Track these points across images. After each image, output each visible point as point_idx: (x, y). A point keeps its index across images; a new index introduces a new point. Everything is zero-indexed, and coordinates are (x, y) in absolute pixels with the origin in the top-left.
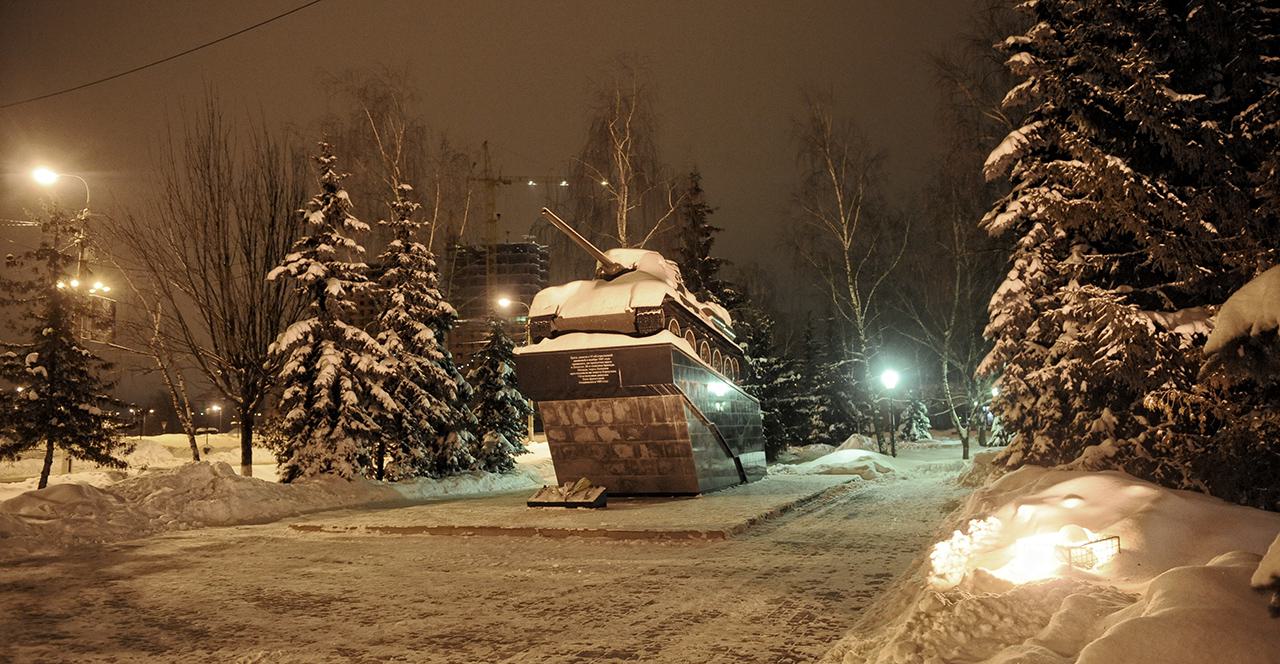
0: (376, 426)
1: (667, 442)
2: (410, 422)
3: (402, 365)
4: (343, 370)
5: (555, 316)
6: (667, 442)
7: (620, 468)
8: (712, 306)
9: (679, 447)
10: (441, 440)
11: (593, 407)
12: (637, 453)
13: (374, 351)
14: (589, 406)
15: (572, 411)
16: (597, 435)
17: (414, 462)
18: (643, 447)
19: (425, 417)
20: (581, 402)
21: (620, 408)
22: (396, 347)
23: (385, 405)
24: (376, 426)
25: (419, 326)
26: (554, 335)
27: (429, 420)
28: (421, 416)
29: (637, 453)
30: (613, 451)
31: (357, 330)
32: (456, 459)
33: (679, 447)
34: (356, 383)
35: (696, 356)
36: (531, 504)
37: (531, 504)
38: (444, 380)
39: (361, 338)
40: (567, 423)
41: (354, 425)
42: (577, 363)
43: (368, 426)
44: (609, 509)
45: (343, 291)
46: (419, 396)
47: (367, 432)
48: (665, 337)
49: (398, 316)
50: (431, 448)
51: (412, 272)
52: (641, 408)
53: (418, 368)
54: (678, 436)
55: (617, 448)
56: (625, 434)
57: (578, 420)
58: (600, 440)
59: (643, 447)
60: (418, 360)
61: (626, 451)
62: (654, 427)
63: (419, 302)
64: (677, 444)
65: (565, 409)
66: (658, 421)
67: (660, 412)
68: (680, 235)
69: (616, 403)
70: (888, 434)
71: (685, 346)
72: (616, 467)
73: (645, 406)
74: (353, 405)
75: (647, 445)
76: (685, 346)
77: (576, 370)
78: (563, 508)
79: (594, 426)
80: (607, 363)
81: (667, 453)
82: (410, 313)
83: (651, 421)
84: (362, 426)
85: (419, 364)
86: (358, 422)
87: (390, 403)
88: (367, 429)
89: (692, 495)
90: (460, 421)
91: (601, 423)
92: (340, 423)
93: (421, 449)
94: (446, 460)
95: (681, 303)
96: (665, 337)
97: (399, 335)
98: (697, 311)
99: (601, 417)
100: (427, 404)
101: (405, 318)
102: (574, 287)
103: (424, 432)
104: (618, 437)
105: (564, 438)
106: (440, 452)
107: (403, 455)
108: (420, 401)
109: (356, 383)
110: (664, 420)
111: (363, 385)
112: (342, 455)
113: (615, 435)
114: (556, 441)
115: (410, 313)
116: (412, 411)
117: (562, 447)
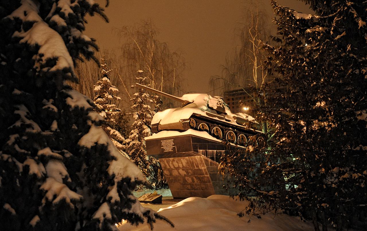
1: (202, 176)
6: (202, 176)
7: (189, 187)
11: (175, 161)
15: (169, 163)
19: (149, 164)
20: (171, 159)
21: (184, 161)
28: (148, 164)
30: (185, 180)
31: (114, 130)
33: (206, 178)
39: (115, 134)
40: (169, 168)
42: (163, 143)
44: (162, 204)
52: (190, 162)
54: (205, 174)
55: (186, 178)
56: (188, 173)
58: (181, 175)
59: (194, 178)
61: (189, 180)
62: (196, 169)
64: (205, 177)
65: (167, 162)
66: (197, 167)
67: (196, 163)
69: (182, 159)
72: (188, 186)
73: (191, 161)
75: (195, 177)
78: (144, 203)
79: (178, 169)
80: (171, 142)
83: (194, 167)
95: (207, 116)
96: (190, 132)
99: (179, 165)
102: (168, 111)
104: (185, 173)
105: (169, 174)
110: (198, 167)
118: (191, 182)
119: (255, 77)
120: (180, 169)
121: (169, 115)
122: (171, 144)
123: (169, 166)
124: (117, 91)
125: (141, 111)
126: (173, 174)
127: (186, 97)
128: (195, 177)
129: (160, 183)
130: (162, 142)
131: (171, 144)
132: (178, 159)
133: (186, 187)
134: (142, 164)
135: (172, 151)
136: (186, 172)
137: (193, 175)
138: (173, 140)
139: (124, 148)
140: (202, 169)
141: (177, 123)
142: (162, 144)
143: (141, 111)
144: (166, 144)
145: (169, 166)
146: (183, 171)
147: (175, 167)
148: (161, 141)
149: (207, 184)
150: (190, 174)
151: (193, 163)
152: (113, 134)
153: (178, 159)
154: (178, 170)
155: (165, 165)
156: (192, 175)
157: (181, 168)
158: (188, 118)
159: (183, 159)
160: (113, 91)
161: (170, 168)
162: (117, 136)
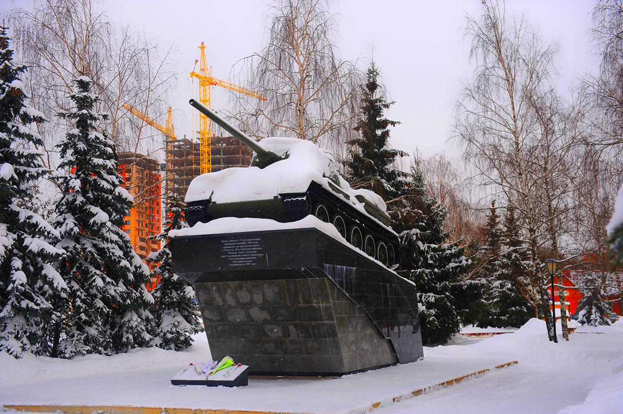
0: (47, 305)
1: (314, 323)
2: (83, 301)
3: (78, 246)
4: (15, 251)
5: (209, 201)
7: (271, 347)
8: (362, 192)
9: (325, 328)
10: (118, 320)
12: (286, 333)
13: (46, 233)
14: (241, 288)
16: (248, 315)
17: (87, 341)
18: (292, 328)
19: (100, 296)
20: (232, 284)
22: (72, 229)
23: (55, 285)
24: (47, 305)
25: (94, 209)
26: (206, 220)
27: (104, 299)
28: (95, 296)
29: (286, 333)
30: (264, 331)
32: (131, 337)
34: (28, 264)
35: (344, 241)
36: (175, 383)
37: (175, 383)
38: (120, 262)
39: (33, 221)
40: (221, 303)
41: (24, 304)
43: (37, 305)
45: (16, 177)
46: (93, 276)
47: (37, 310)
48: (310, 221)
49: (75, 200)
50: (108, 327)
51: (90, 159)
53: (93, 250)
55: (267, 328)
57: (231, 302)
59: (292, 328)
60: (95, 242)
63: (96, 187)
68: (95, 100)
70: (397, 327)
71: (330, 229)
72: (267, 346)
74: (22, 285)
75: (296, 326)
76: (330, 229)
77: (226, 253)
81: (314, 334)
82: (88, 198)
83: (298, 302)
84: (32, 305)
85: (95, 246)
86: (27, 301)
87: (60, 282)
88: (35, 307)
89: (339, 375)
90: (136, 300)
91: (252, 304)
92: (10, 302)
93: (95, 326)
94: (122, 337)
95: (330, 189)
96: (310, 221)
97: (76, 219)
98: (347, 197)
99: (252, 298)
100: (99, 282)
101: (82, 202)
103: (98, 311)
105: (218, 318)
106: (117, 329)
107: (76, 333)
108: (94, 281)
109: (28, 264)
110: (310, 302)
111: (35, 265)
112: (11, 333)
113: (265, 315)
114: (211, 320)
115: (88, 198)
116: (87, 291)
117: (216, 328)
118: (279, 337)
122: (254, 249)
123: (224, 300)
125: (82, 173)
131: (254, 249)
132: (253, 283)
134: (85, 296)
136: (270, 313)
140: (319, 308)
142: (225, 247)
143: (82, 173)
145: (224, 300)
146: (263, 310)
150: (280, 318)
152: (25, 221)
154: (248, 308)
161: (224, 305)
162: (39, 227)
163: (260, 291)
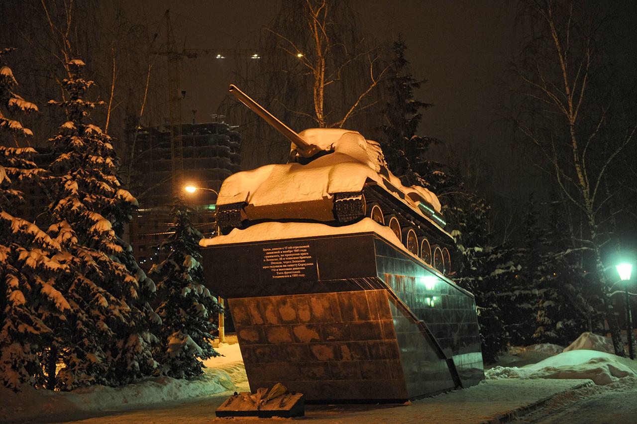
0: (46, 329)
1: (371, 342)
2: (86, 324)
3: (76, 260)
4: (9, 267)
5: (245, 204)
6: (371, 342)
7: (319, 371)
8: (419, 190)
9: (384, 348)
10: (120, 344)
11: (289, 304)
12: (338, 354)
13: (44, 245)
14: (284, 303)
15: (265, 308)
16: (293, 335)
17: (90, 369)
18: (344, 348)
19: (102, 317)
20: (274, 299)
21: (319, 304)
22: (69, 240)
23: (58, 305)
24: (46, 329)
25: (95, 217)
26: (244, 225)
27: (107, 321)
28: (98, 317)
29: (338, 354)
30: (311, 352)
31: (25, 223)
32: (137, 364)
33: (384, 348)
34: (24, 281)
35: (402, 247)
36: (220, 414)
37: (220, 414)
38: (124, 277)
39: (30, 231)
40: (260, 321)
41: (21, 329)
42: (270, 255)
43: (37, 329)
44: (306, 418)
45: (9, 180)
46: (95, 294)
47: (37, 335)
48: (367, 225)
49: (72, 205)
50: (109, 353)
51: (87, 157)
52: (342, 305)
53: (94, 264)
54: (383, 337)
55: (315, 349)
56: (324, 334)
57: (272, 318)
58: (297, 340)
59: (344, 348)
60: (95, 254)
61: (325, 353)
62: (356, 325)
63: (96, 189)
64: (382, 344)
65: (258, 306)
66: (360, 318)
67: (362, 308)
68: (383, 112)
69: (314, 299)
70: (625, 332)
71: (389, 235)
73: (346, 302)
74: (21, 306)
75: (349, 346)
76: (389, 235)
77: (269, 264)
78: (256, 418)
79: (290, 325)
80: (303, 254)
81: (371, 355)
82: (85, 203)
83: (352, 318)
84: (30, 329)
85: (96, 259)
86: (26, 325)
87: (62, 302)
88: (35, 332)
89: (401, 402)
90: (141, 321)
91: (297, 321)
92: (6, 327)
93: (97, 353)
94: (126, 365)
95: (385, 188)
96: (367, 225)
97: (72, 227)
98: (402, 195)
99: (297, 315)
100: (104, 302)
101: (79, 208)
102: (266, 172)
103: (102, 334)
104: (317, 336)
105: (257, 339)
106: (119, 356)
107: (78, 361)
108: (97, 300)
109: (24, 281)
110: (366, 317)
111: (32, 283)
112: (7, 363)
113: (314, 334)
114: (248, 342)
115: (85, 203)
116: (88, 312)
117: (255, 350)
118: (330, 359)
119: (319, 108)
120: (297, 326)
121: (271, 184)
122: (302, 258)
123: (263, 317)
124: (33, 109)
125: (78, 173)
126: (270, 340)
127: (312, 137)
128: (347, 344)
129: (112, 371)
130: (268, 253)
131: (302, 258)
132: (299, 298)
133: (310, 373)
134: (86, 317)
135: (303, 275)
136: (318, 331)
137: (343, 340)
138: (308, 246)
139: (67, 271)
140: (378, 324)
141: (317, 201)
142: (267, 257)
143: (78, 173)
144: (281, 259)
145: (263, 317)
146: (311, 329)
147: (284, 319)
148: (264, 250)
149: (385, 363)
150: (331, 338)
151: (351, 308)
152: (19, 231)
153: (299, 298)
154: (293, 327)
155: (247, 315)
156: (339, 340)
157: (304, 323)
158: (359, 188)
159: (318, 298)
160: (23, 109)
161: (264, 324)
162: (36, 238)
163: (308, 306)
